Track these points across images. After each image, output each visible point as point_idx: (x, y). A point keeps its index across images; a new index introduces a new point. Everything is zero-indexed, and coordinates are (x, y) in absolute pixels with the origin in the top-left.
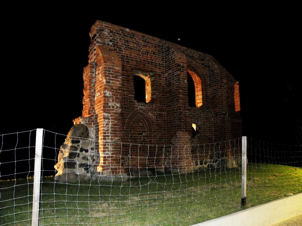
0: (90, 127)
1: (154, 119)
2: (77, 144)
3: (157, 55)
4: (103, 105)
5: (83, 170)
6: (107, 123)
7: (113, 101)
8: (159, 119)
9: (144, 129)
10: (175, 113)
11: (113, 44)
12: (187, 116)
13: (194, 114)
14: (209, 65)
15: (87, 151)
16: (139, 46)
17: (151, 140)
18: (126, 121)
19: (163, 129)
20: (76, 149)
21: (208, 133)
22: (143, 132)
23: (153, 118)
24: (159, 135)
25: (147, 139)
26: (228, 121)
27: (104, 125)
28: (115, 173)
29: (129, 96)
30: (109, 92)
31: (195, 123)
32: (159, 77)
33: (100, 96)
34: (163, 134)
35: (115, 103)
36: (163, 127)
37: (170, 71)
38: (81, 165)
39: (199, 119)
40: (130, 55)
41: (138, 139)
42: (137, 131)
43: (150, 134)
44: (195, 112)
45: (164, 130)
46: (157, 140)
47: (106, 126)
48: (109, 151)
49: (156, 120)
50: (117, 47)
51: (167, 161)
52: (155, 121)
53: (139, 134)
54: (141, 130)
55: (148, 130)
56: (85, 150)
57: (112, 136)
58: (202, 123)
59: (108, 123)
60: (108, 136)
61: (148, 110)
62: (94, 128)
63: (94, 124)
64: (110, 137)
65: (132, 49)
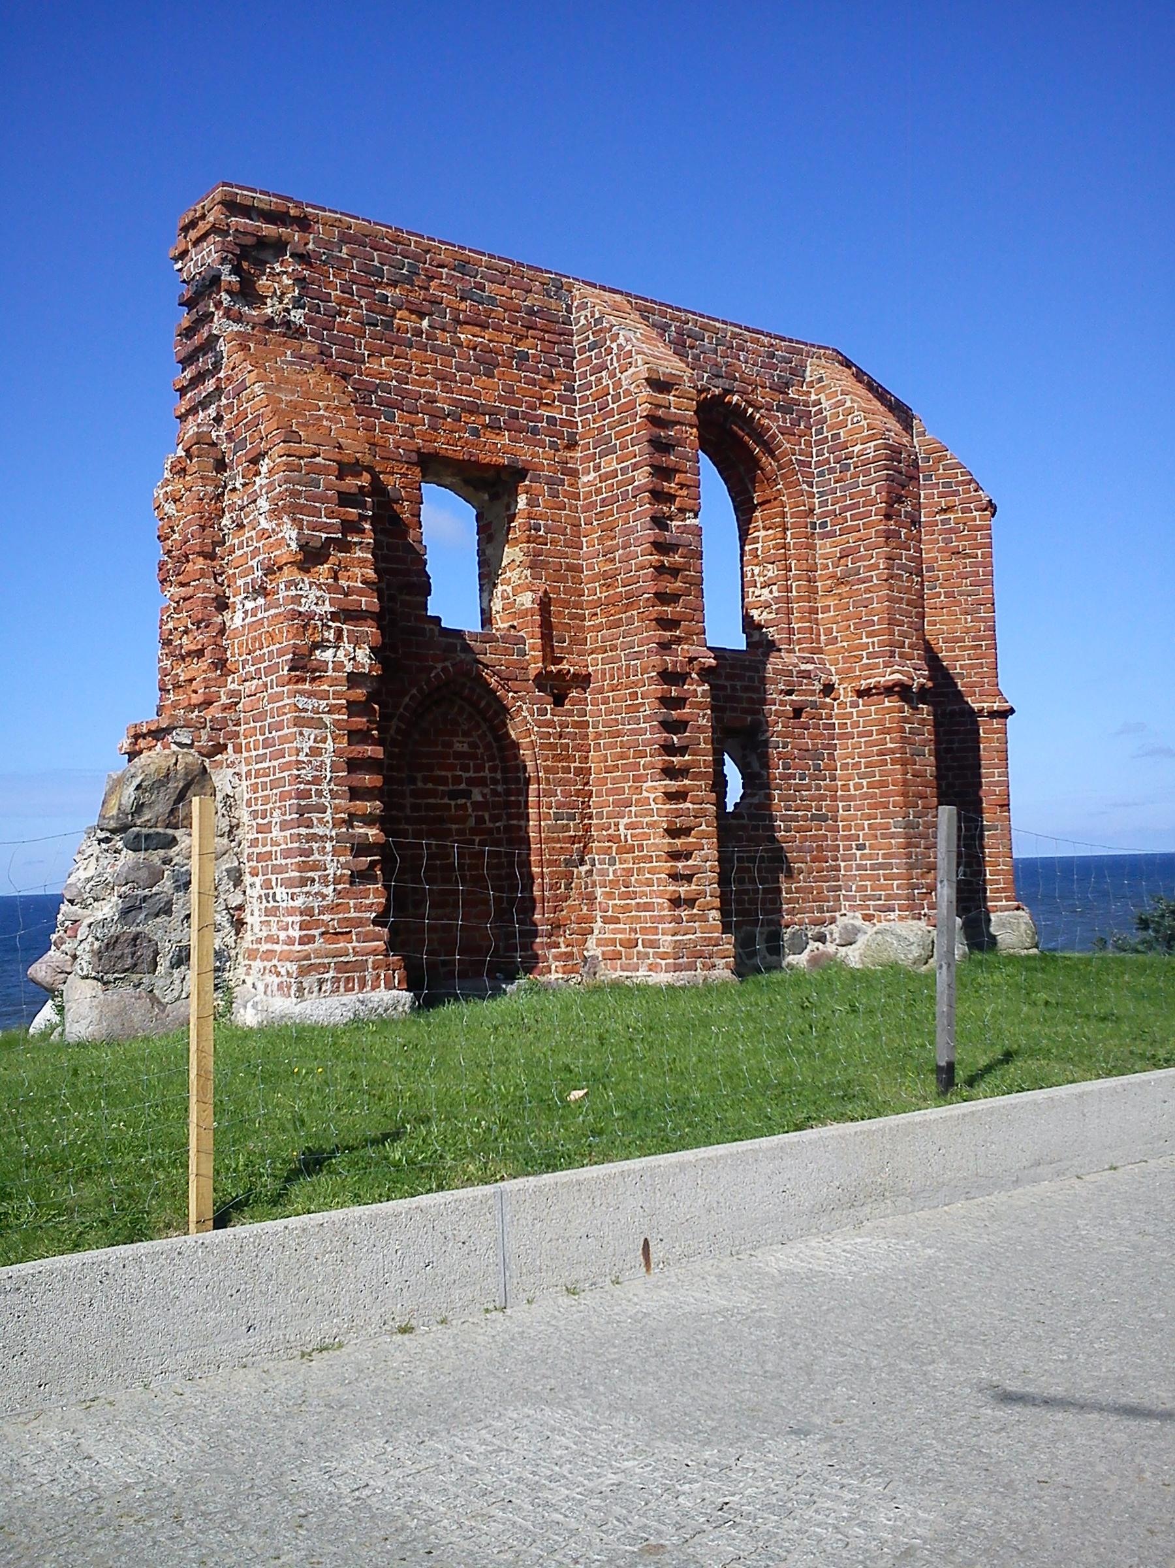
0: (219, 765)
2: (162, 852)
4: (291, 656)
6: (311, 743)
8: (556, 719)
10: (635, 684)
11: (310, 320)
13: (734, 688)
14: (820, 411)
17: (514, 822)
18: (392, 732)
19: (572, 765)
20: (157, 877)
22: (471, 782)
27: (302, 757)
30: (315, 593)
33: (272, 611)
37: (609, 464)
40: (403, 380)
41: (455, 820)
42: (443, 781)
43: (508, 793)
44: (741, 677)
45: (579, 771)
47: (310, 762)
51: (596, 932)
52: (536, 729)
53: (454, 795)
54: (465, 775)
55: (499, 776)
57: (337, 810)
59: (321, 745)
62: (236, 770)
63: (238, 750)
64: (328, 816)
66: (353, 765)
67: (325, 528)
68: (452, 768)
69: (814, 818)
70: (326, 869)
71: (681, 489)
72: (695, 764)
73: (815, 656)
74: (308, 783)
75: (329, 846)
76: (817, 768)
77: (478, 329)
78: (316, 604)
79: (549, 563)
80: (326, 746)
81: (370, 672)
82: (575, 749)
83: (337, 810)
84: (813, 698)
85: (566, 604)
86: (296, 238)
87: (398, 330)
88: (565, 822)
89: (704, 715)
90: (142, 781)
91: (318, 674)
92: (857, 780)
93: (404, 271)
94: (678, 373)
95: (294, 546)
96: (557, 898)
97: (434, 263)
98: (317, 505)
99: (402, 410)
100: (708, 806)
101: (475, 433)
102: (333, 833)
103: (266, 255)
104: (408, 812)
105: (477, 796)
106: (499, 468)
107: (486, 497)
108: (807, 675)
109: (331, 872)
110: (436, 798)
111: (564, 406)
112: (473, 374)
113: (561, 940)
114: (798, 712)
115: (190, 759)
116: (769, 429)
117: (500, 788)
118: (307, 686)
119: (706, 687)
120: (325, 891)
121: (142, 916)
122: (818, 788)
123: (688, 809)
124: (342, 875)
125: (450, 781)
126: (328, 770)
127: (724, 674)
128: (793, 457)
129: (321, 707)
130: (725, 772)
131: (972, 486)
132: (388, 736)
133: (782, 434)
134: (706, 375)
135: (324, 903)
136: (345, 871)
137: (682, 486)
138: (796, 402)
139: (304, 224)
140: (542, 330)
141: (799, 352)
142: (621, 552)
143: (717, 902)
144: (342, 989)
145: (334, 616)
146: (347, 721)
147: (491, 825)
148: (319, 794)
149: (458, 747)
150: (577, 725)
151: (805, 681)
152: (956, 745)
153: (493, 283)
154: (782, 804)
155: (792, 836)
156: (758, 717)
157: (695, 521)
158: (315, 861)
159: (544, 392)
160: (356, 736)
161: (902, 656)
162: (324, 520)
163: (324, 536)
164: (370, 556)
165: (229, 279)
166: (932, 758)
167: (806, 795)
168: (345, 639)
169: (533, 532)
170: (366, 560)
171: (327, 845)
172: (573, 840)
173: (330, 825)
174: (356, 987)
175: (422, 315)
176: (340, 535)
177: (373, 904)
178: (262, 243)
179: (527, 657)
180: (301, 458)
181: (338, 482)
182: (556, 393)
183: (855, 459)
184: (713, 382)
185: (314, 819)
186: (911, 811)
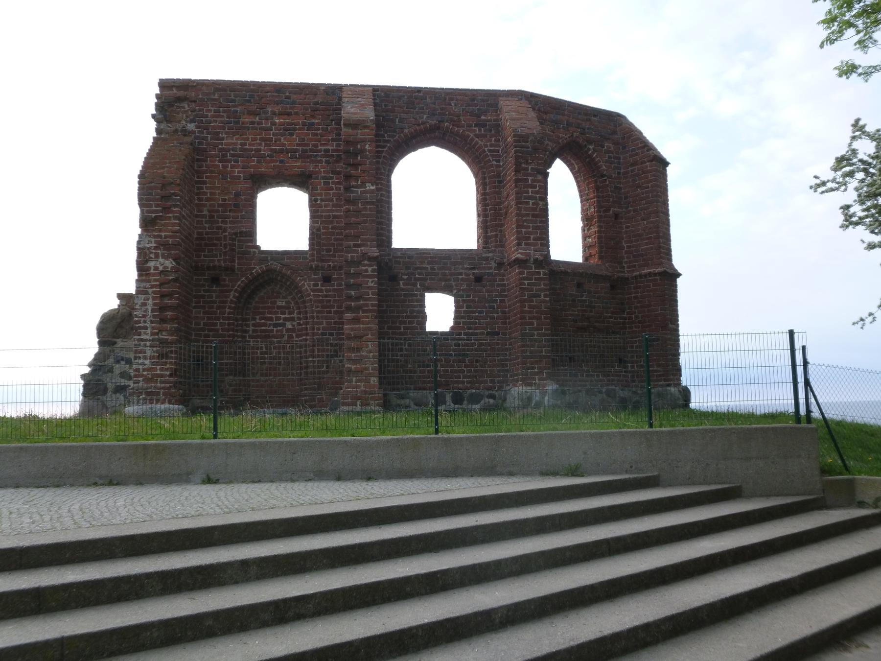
1: (308, 288)
3: (319, 129)
6: (142, 301)
8: (323, 288)
9: (292, 313)
11: (197, 127)
12: (370, 273)
13: (432, 269)
15: (129, 361)
16: (267, 119)
18: (231, 297)
21: (485, 318)
22: (285, 319)
24: (321, 326)
26: (536, 279)
27: (137, 307)
28: (154, 402)
32: (326, 183)
34: (335, 323)
35: (161, 260)
36: (333, 307)
39: (449, 280)
42: (271, 319)
45: (335, 312)
46: (315, 337)
48: (145, 358)
50: (208, 133)
52: (312, 293)
53: (276, 325)
56: (122, 359)
57: (153, 328)
58: (463, 290)
59: (146, 302)
60: (146, 328)
61: (291, 268)
64: (149, 331)
65: (248, 129)
66: (162, 309)
68: (276, 313)
69: (488, 334)
70: (146, 353)
71: (364, 173)
72: (367, 305)
73: (497, 249)
74: (140, 317)
75: (148, 343)
76: (493, 307)
77: (286, 116)
78: (148, 244)
79: (322, 215)
81: (171, 269)
82: (335, 301)
83: (153, 328)
84: (490, 271)
86: (193, 95)
89: (372, 282)
93: (247, 98)
94: (364, 119)
96: (323, 372)
100: (372, 326)
102: (151, 339)
104: (251, 332)
105: (289, 325)
109: (149, 353)
111: (335, 143)
112: (282, 136)
114: (478, 279)
115: (125, 311)
116: (468, 136)
117: (301, 322)
120: (146, 362)
121: (101, 373)
122: (493, 318)
124: (154, 356)
125: (274, 319)
126: (150, 312)
127: (426, 262)
128: (486, 149)
132: (229, 299)
134: (425, 116)
135: (145, 367)
136: (155, 354)
137: (363, 171)
138: (490, 121)
140: (323, 111)
143: (377, 373)
144: (148, 403)
145: (156, 248)
146: (159, 291)
147: (297, 339)
148: (145, 322)
149: (279, 303)
150: (335, 290)
152: (639, 295)
154: (466, 326)
155: (472, 343)
156: (450, 282)
160: (163, 296)
161: (526, 244)
163: (153, 215)
168: (160, 257)
172: (332, 345)
173: (150, 335)
174: (154, 402)
176: (161, 214)
177: (168, 368)
179: (308, 260)
182: (330, 138)
185: (142, 333)
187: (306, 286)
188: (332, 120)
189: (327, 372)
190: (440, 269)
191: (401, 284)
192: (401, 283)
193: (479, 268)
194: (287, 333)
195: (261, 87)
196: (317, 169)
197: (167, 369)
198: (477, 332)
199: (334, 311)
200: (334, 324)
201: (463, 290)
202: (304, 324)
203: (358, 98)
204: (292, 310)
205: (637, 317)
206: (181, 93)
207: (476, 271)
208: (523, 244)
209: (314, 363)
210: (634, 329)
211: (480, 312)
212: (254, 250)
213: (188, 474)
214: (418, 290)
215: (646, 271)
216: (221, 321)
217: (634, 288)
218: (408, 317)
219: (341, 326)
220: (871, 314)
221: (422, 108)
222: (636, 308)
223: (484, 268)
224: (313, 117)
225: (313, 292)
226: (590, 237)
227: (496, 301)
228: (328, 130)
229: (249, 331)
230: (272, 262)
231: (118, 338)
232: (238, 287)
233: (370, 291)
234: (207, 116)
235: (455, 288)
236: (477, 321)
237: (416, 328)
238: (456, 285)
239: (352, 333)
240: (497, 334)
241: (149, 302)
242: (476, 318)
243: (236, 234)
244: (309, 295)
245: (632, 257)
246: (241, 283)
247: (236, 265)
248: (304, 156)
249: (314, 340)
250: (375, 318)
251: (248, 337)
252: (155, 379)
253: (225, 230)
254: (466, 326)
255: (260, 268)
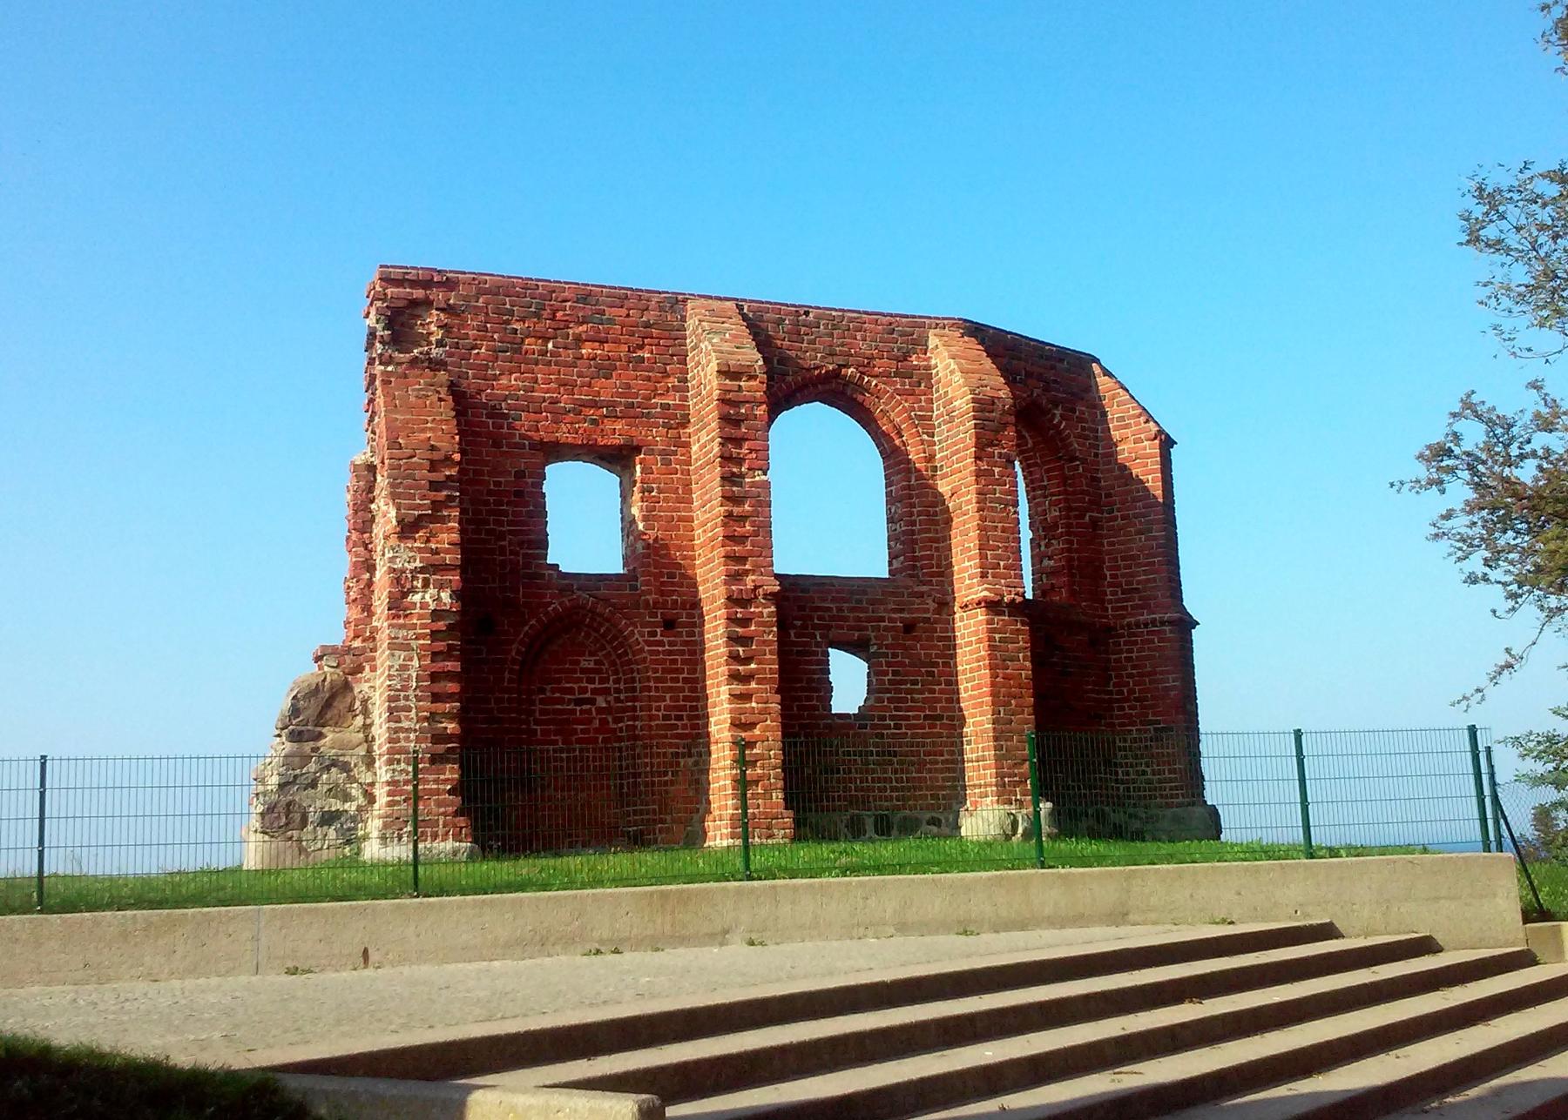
0: (359, 681)
1: (640, 639)
2: (311, 744)
5: (332, 833)
6: (401, 662)
7: (426, 585)
8: (665, 640)
13: (840, 609)
19: (681, 676)
20: (306, 759)
22: (594, 691)
23: (637, 636)
25: (617, 720)
29: (525, 555)
31: (856, 647)
34: (686, 699)
36: (681, 671)
38: (328, 818)
39: (866, 629)
41: (580, 722)
46: (653, 723)
49: (643, 641)
52: (646, 648)
53: (579, 702)
58: (887, 647)
61: (613, 605)
62: (371, 684)
64: (413, 714)
66: (434, 677)
67: (418, 507)
68: (580, 680)
69: (926, 717)
74: (398, 690)
75: (412, 736)
76: (931, 674)
77: (598, 344)
78: (409, 562)
80: (413, 663)
81: (451, 608)
82: (684, 662)
85: (680, 548)
87: (526, 353)
88: (673, 722)
90: (298, 693)
91: (408, 612)
92: (966, 685)
94: (749, 363)
95: (394, 522)
97: (559, 300)
98: (412, 491)
99: (528, 412)
100: (773, 705)
101: (594, 422)
102: (417, 727)
103: (418, 311)
106: (620, 448)
107: (619, 468)
108: (922, 595)
110: (562, 705)
111: (678, 394)
113: (668, 818)
114: (909, 627)
117: (622, 696)
118: (401, 621)
119: (773, 609)
122: (933, 692)
123: (753, 708)
129: (409, 636)
130: (831, 680)
131: (1142, 419)
133: (900, 395)
134: (819, 355)
138: (918, 368)
139: (449, 284)
141: (923, 325)
142: (709, 505)
143: (780, 784)
145: (422, 570)
148: (407, 698)
149: (584, 664)
150: (686, 643)
151: (918, 601)
152: (1134, 655)
153: (612, 307)
154: (892, 706)
157: (763, 477)
158: (400, 747)
159: (658, 385)
162: (418, 501)
163: (416, 513)
164: (457, 525)
165: (382, 333)
166: (1028, 664)
167: (919, 698)
168: (431, 586)
169: (646, 494)
170: (453, 528)
171: (411, 735)
173: (415, 720)
175: (546, 339)
176: (430, 512)
177: (448, 780)
178: (414, 303)
180: (402, 459)
181: (430, 474)
182: (670, 385)
183: (957, 412)
184: (826, 360)
185: (403, 718)
186: (1002, 709)
187: (637, 636)
188: (672, 355)
189: (672, 783)
190: (852, 609)
191: (792, 635)
192: (792, 633)
193: (911, 611)
194: (599, 716)
195: (554, 292)
196: (650, 438)
197: (447, 780)
198: (909, 716)
199: (683, 678)
200: (683, 701)
201: (887, 647)
202: (628, 699)
203: (723, 323)
204: (605, 675)
205: (1131, 692)
206: (419, 293)
207: (908, 616)
208: (989, 575)
209: (652, 767)
210: (1127, 711)
211: (915, 683)
212: (550, 572)
213: (726, 932)
214: (818, 645)
215: (1146, 617)
216: (497, 695)
217: (1126, 643)
218: (803, 689)
219: (694, 704)
220: (1478, 690)
221: (813, 342)
222: (1130, 676)
223: (918, 610)
224: (641, 347)
225: (648, 646)
226: (1050, 558)
227: (936, 665)
228: (666, 372)
229: (534, 711)
230: (580, 593)
231: (324, 727)
232: (524, 636)
233: (767, 649)
234: (466, 336)
235: (874, 641)
236: (909, 696)
237: (815, 708)
238: (875, 637)
239: (742, 716)
240: (940, 718)
241: (413, 663)
242: (908, 692)
243: (521, 544)
244: (642, 650)
245: (1120, 592)
246: (530, 628)
247: (521, 596)
248: (632, 413)
249: (650, 727)
250: (776, 693)
251: (532, 723)
252: (426, 797)
253: (502, 536)
254: (892, 706)
255: (560, 604)
